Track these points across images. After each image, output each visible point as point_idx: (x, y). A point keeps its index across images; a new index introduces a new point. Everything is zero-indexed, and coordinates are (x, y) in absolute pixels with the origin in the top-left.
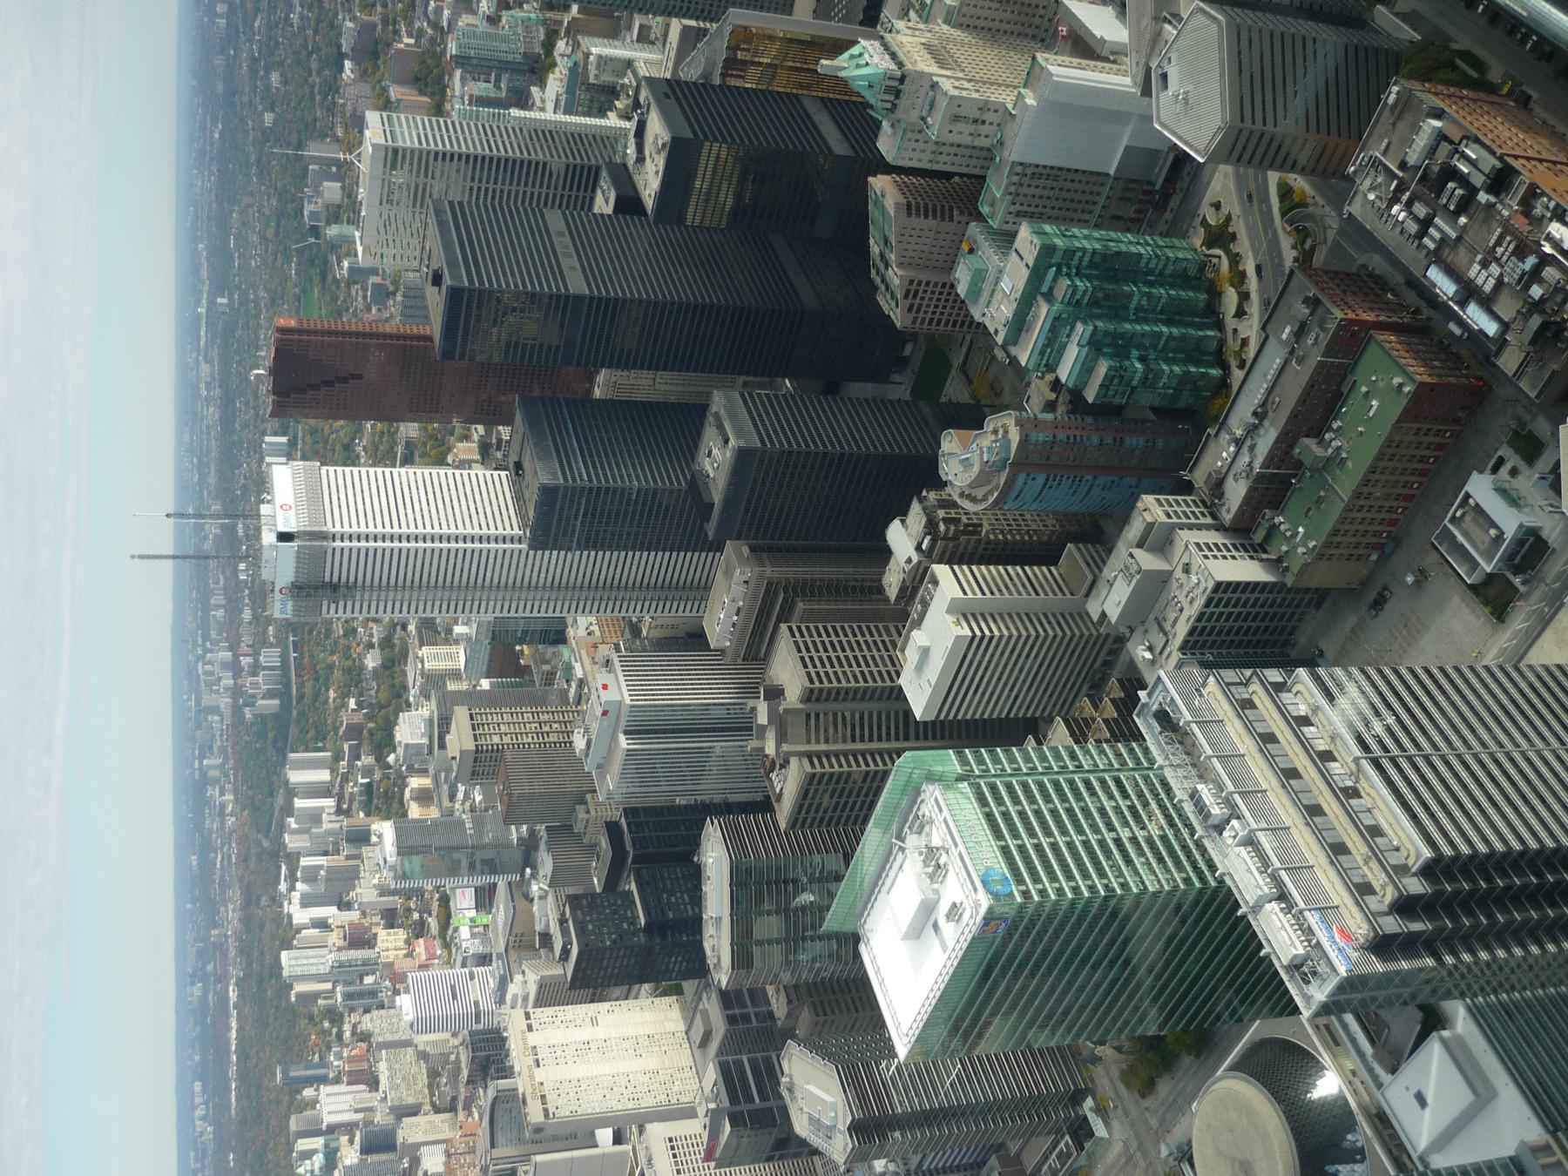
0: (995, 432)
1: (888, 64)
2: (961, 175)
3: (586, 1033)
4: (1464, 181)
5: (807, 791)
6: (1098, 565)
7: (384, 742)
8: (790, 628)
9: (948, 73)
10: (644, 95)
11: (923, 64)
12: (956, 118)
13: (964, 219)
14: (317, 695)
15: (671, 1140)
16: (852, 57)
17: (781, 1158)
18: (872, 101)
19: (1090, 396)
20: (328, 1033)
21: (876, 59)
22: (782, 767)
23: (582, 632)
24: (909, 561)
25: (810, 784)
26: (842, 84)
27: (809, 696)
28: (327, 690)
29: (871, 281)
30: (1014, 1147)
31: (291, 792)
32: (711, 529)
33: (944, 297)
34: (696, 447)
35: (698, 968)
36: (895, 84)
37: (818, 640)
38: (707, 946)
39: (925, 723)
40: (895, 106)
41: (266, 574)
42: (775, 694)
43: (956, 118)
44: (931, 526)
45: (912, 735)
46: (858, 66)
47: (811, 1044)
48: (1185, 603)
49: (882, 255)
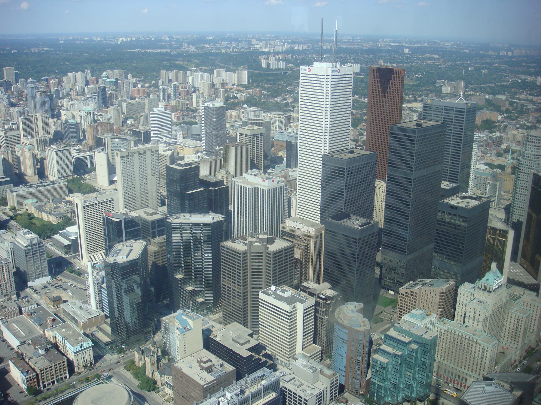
0: (363, 322)
1: (495, 286)
2: (454, 312)
3: (149, 171)
5: (235, 252)
6: (313, 357)
7: (251, 102)
8: (293, 247)
10: (484, 200)
13: (439, 312)
14: (269, 80)
15: (113, 200)
17: (105, 239)
18: (481, 281)
20: (150, 83)
21: (497, 282)
22: (244, 243)
23: (290, 173)
25: (237, 253)
26: (488, 269)
28: (270, 84)
29: (417, 280)
30: (108, 320)
31: (234, 71)
33: (411, 305)
34: (358, 215)
35: (171, 213)
36: (488, 289)
37: (289, 257)
38: (181, 215)
39: (258, 295)
40: (480, 289)
41: (315, 64)
42: (270, 241)
44: (328, 298)
45: (253, 290)
47: (145, 252)
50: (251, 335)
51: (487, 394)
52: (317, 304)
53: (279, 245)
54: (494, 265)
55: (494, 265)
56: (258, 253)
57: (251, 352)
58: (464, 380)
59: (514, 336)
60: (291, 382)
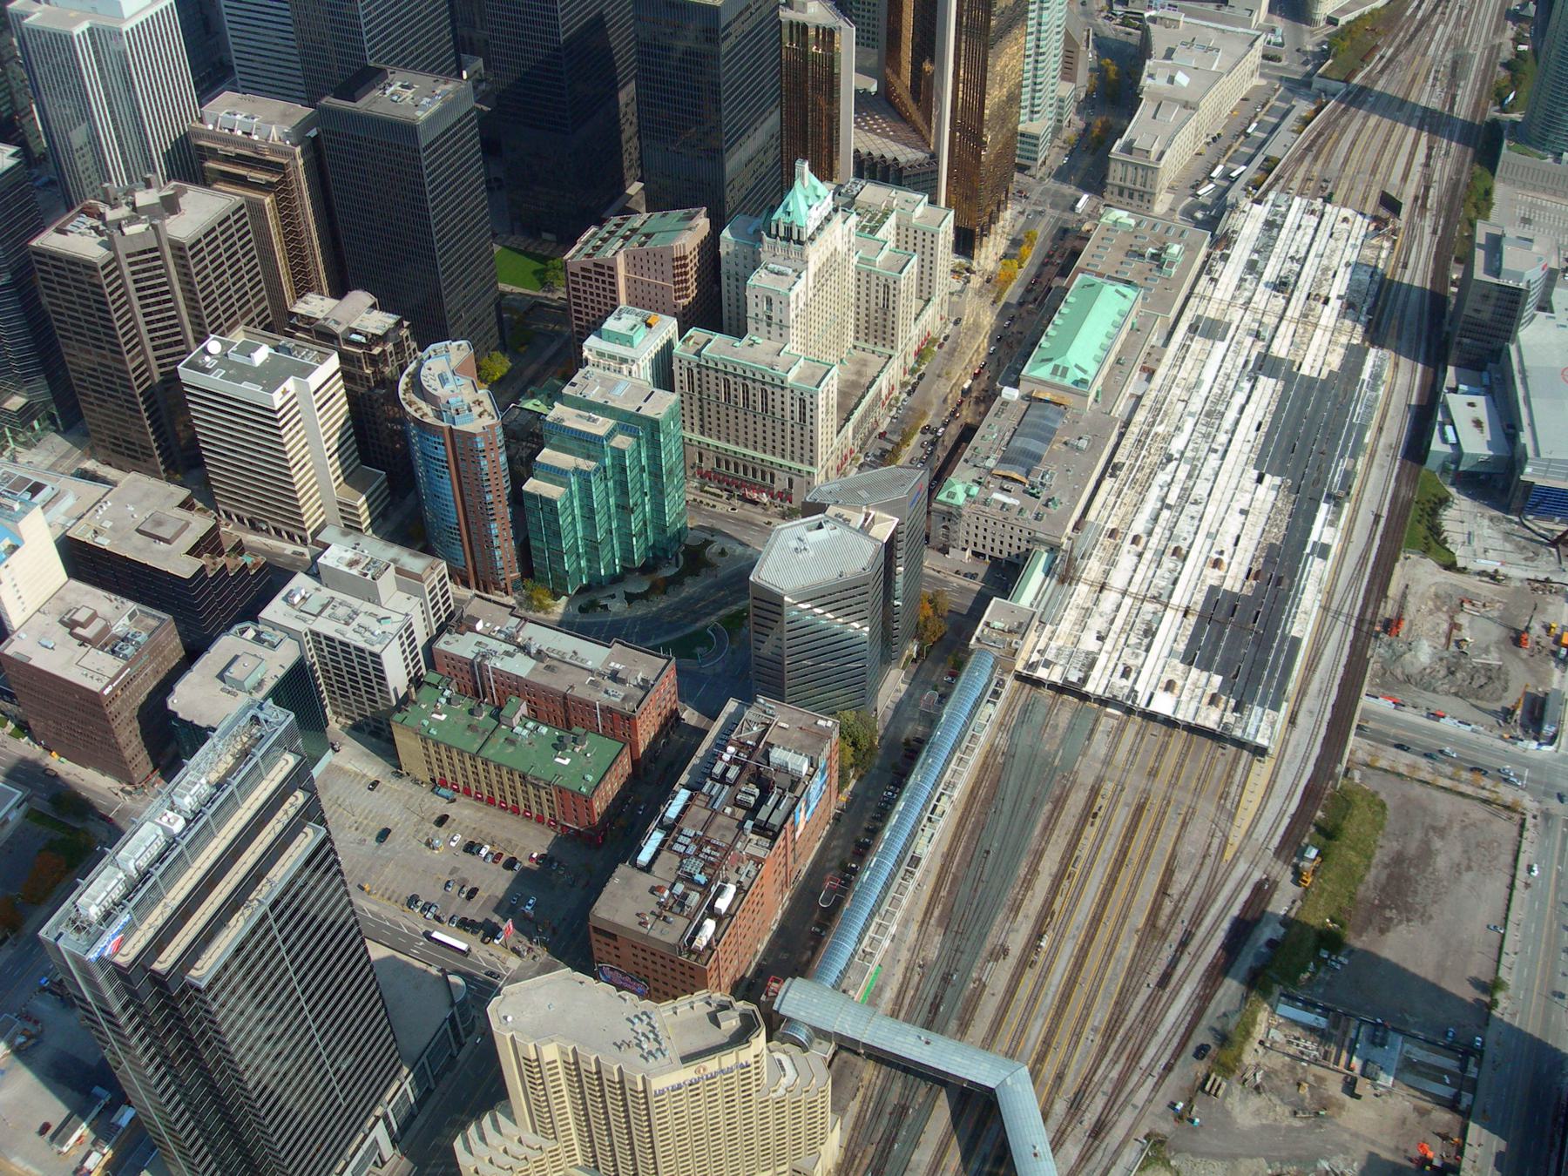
4: (761, 801)
9: (811, 284)
11: (816, 255)
12: (769, 301)
16: (815, 188)
19: (531, 485)
24: (337, 323)
26: (786, 182)
27: (178, 248)
29: (605, 220)
32: (329, 101)
36: (795, 237)
42: (170, 205)
43: (769, 301)
44: (376, 339)
45: (159, 353)
46: (807, 197)
48: (354, 624)
49: (634, 231)
50: (186, 505)
51: (812, 553)
52: (344, 357)
53: (200, 211)
54: (803, 167)
55: (803, 167)
56: (144, 252)
57: (199, 556)
58: (768, 477)
59: (880, 328)
60: (325, 614)
